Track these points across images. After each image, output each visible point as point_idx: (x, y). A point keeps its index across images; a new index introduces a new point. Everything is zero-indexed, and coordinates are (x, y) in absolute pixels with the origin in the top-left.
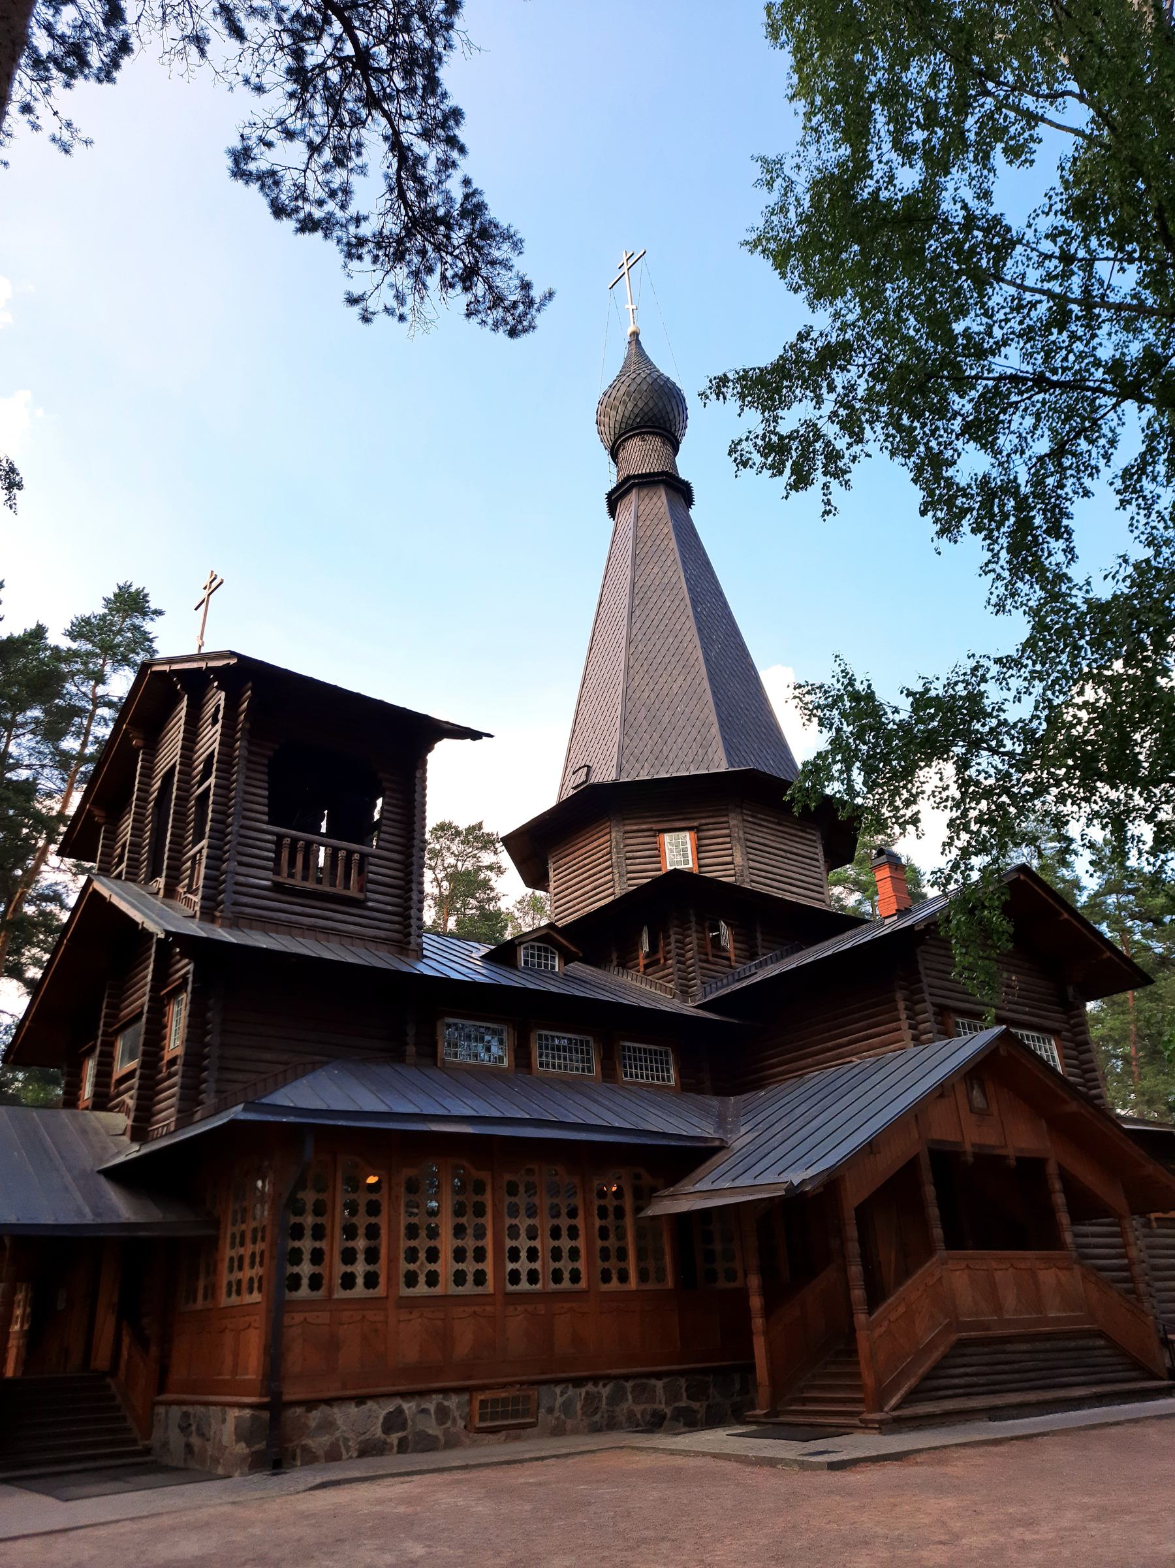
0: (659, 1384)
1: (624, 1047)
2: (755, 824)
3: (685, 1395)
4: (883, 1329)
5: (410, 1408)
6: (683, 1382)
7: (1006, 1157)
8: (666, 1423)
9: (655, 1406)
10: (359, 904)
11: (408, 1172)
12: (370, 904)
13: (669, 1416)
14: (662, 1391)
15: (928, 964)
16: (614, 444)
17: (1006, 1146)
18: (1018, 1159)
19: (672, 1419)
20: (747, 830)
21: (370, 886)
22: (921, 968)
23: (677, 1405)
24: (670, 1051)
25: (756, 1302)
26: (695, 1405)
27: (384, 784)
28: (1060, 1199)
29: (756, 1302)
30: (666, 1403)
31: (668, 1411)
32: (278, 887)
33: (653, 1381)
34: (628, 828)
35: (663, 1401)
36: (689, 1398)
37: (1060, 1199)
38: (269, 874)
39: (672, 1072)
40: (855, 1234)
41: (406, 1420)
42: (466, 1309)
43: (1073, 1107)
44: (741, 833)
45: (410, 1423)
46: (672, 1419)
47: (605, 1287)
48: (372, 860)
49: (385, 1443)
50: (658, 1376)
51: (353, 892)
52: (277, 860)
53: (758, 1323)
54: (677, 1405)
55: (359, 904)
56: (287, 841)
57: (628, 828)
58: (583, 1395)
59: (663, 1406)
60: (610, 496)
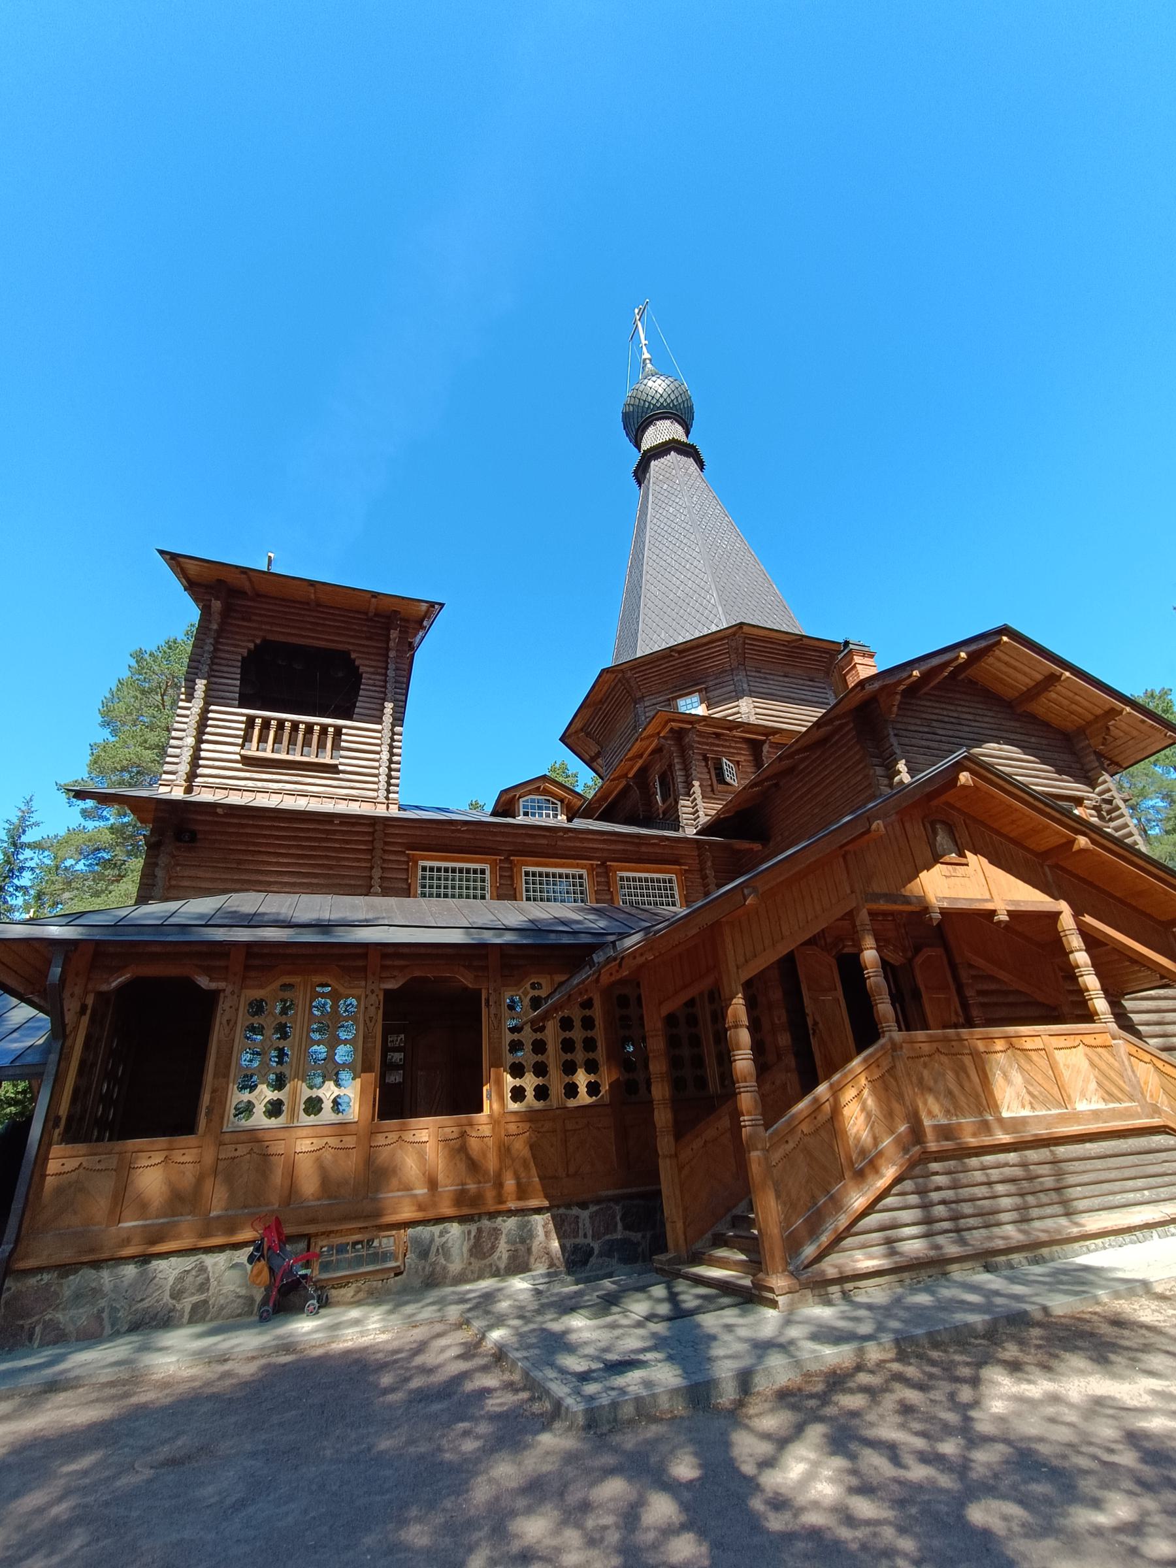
0: (585, 1215)
1: (622, 879)
2: (760, 678)
3: (620, 1226)
4: (791, 1145)
5: (215, 1264)
6: (618, 1209)
7: (993, 913)
8: (593, 1260)
9: (580, 1240)
10: (333, 769)
11: (258, 994)
12: (341, 768)
13: (596, 1252)
14: (587, 1222)
15: (906, 741)
16: (636, 436)
17: (991, 900)
18: (1010, 913)
19: (600, 1255)
20: (751, 683)
21: (343, 753)
22: (894, 740)
23: (608, 1237)
24: (674, 877)
25: (662, 1117)
26: (636, 1236)
27: (362, 669)
28: (1081, 958)
29: (662, 1117)
30: (593, 1237)
31: (596, 1246)
32: (248, 761)
33: (575, 1211)
34: (647, 704)
35: (590, 1233)
36: (627, 1227)
37: (1081, 958)
38: (237, 749)
39: (677, 897)
40: (744, 1019)
41: (208, 1279)
42: (315, 1140)
43: (1082, 841)
44: (745, 686)
45: (213, 1283)
46: (600, 1255)
47: (572, 1103)
48: (344, 731)
49: (173, 1310)
50: (583, 1205)
51: (326, 759)
52: (247, 738)
53: (665, 1143)
54: (608, 1237)
55: (333, 769)
56: (259, 721)
57: (647, 704)
58: (473, 1234)
59: (589, 1240)
60: (636, 473)
